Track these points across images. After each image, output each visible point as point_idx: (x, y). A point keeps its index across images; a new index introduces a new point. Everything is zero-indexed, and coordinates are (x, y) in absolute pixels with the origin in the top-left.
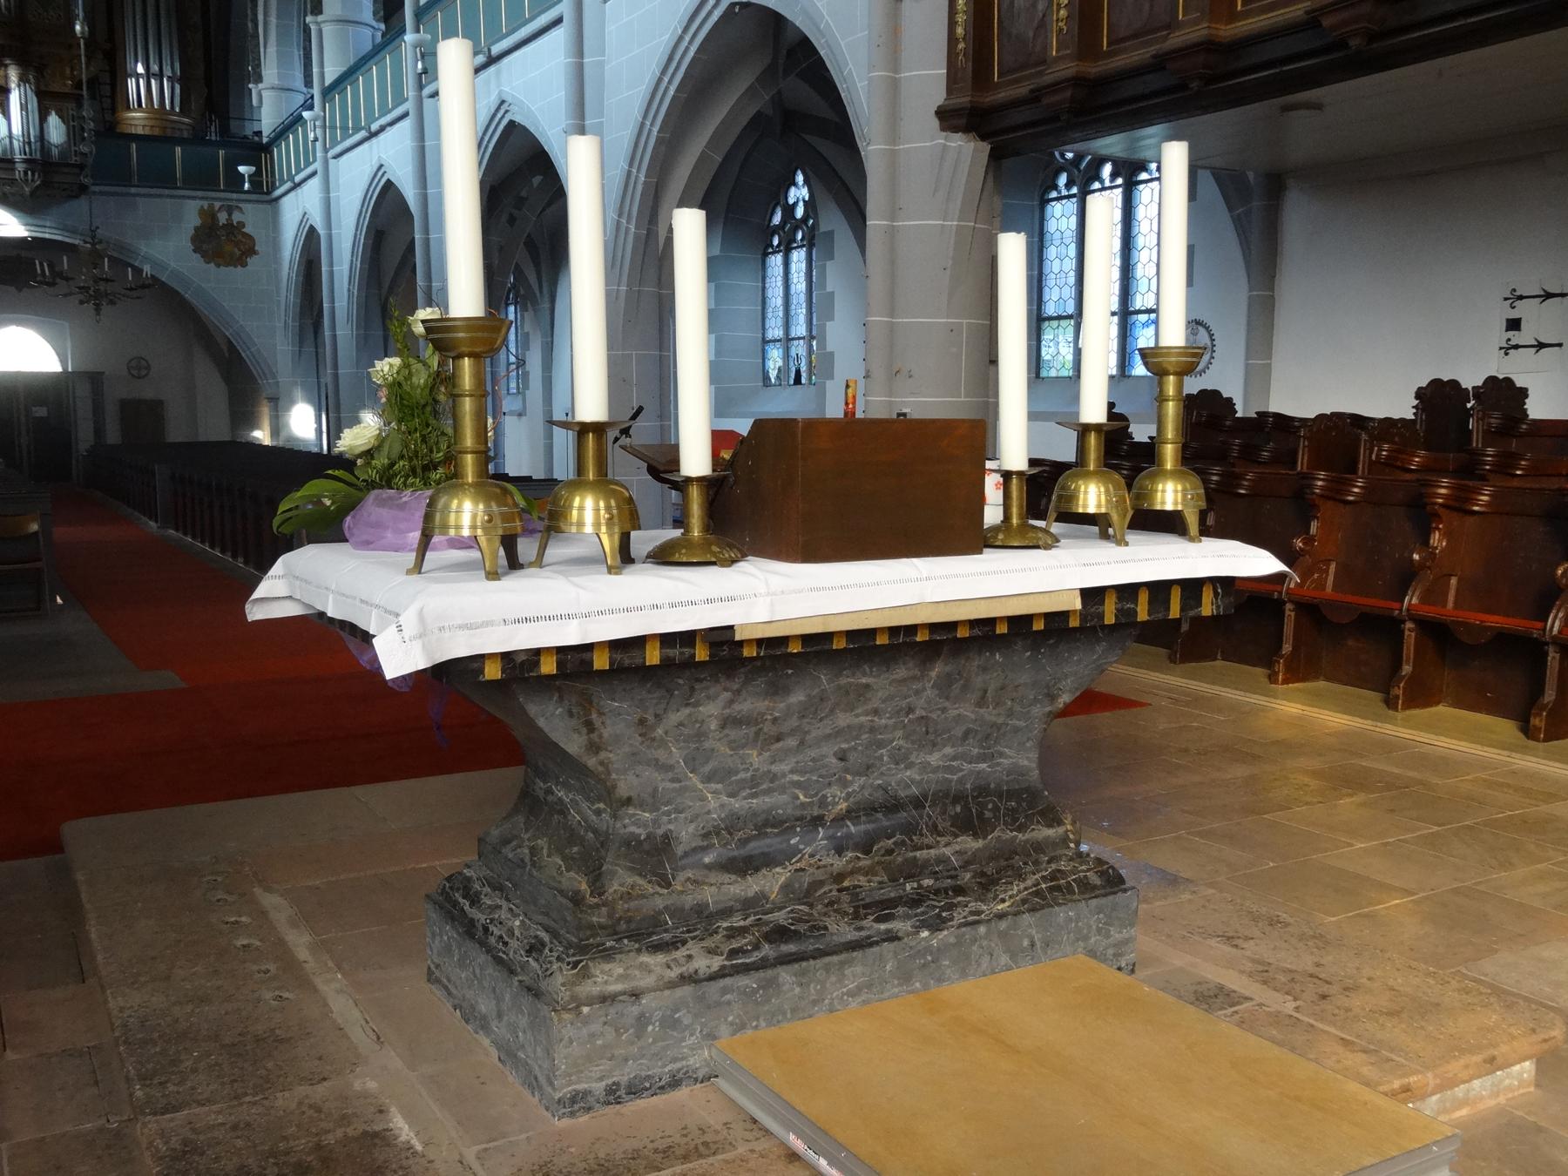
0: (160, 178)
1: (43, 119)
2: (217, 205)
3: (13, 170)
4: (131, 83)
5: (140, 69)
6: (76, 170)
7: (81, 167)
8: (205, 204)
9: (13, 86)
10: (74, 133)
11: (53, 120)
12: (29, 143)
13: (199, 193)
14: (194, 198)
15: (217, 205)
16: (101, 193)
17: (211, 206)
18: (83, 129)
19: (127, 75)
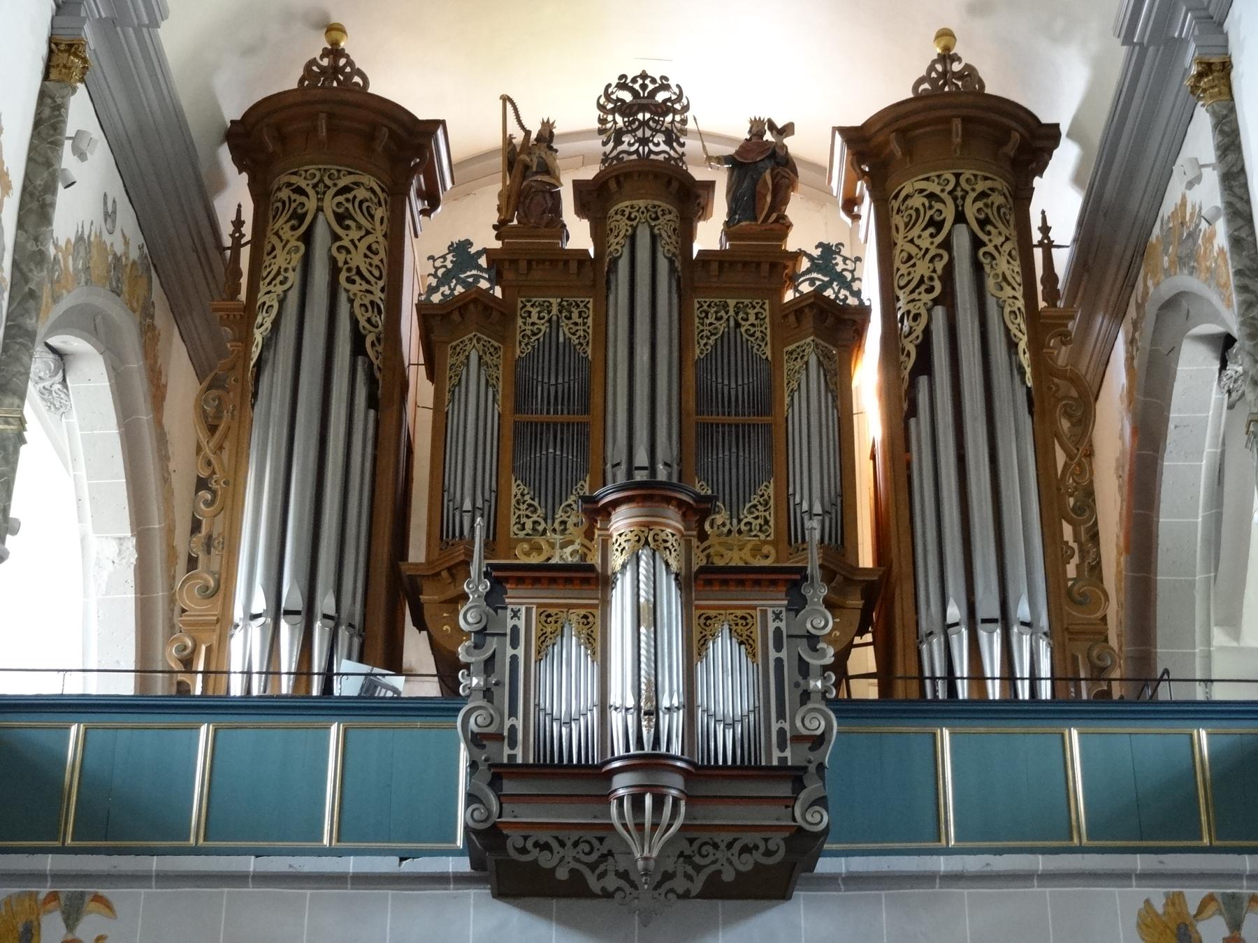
0: (1022, 823)
1: (695, 649)
2: (1194, 896)
3: (605, 798)
4: (933, 653)
5: (954, 612)
6: (784, 790)
7: (795, 776)
8: (1157, 895)
9: (617, 560)
10: (782, 687)
11: (723, 649)
12: (654, 713)
13: (1139, 862)
14: (1121, 877)
15: (1194, 896)
16: (855, 880)
17: (1175, 901)
18: (804, 669)
19: (919, 638)
